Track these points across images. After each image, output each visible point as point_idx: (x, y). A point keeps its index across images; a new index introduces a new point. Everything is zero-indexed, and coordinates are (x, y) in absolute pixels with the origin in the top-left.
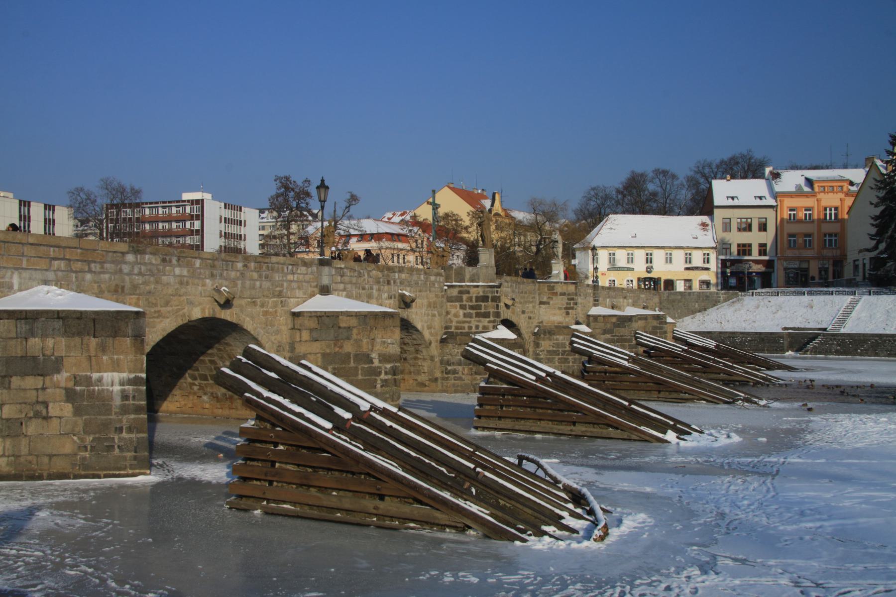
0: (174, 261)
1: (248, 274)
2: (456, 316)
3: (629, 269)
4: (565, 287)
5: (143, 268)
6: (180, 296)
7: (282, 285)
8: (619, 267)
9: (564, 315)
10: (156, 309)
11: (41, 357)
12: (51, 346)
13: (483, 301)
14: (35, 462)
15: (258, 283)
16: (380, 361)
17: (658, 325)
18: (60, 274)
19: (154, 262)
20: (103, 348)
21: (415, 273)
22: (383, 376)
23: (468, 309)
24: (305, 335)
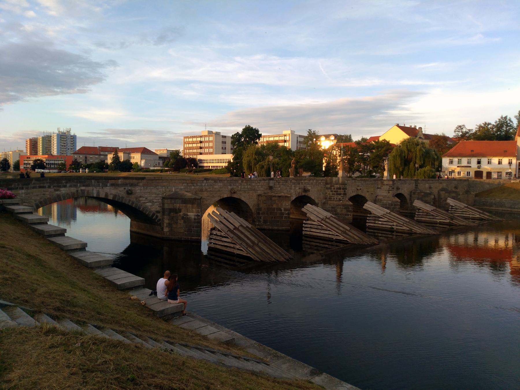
2: (329, 194)
7: (255, 187)
9: (388, 193)
15: (246, 187)
22: (285, 215)
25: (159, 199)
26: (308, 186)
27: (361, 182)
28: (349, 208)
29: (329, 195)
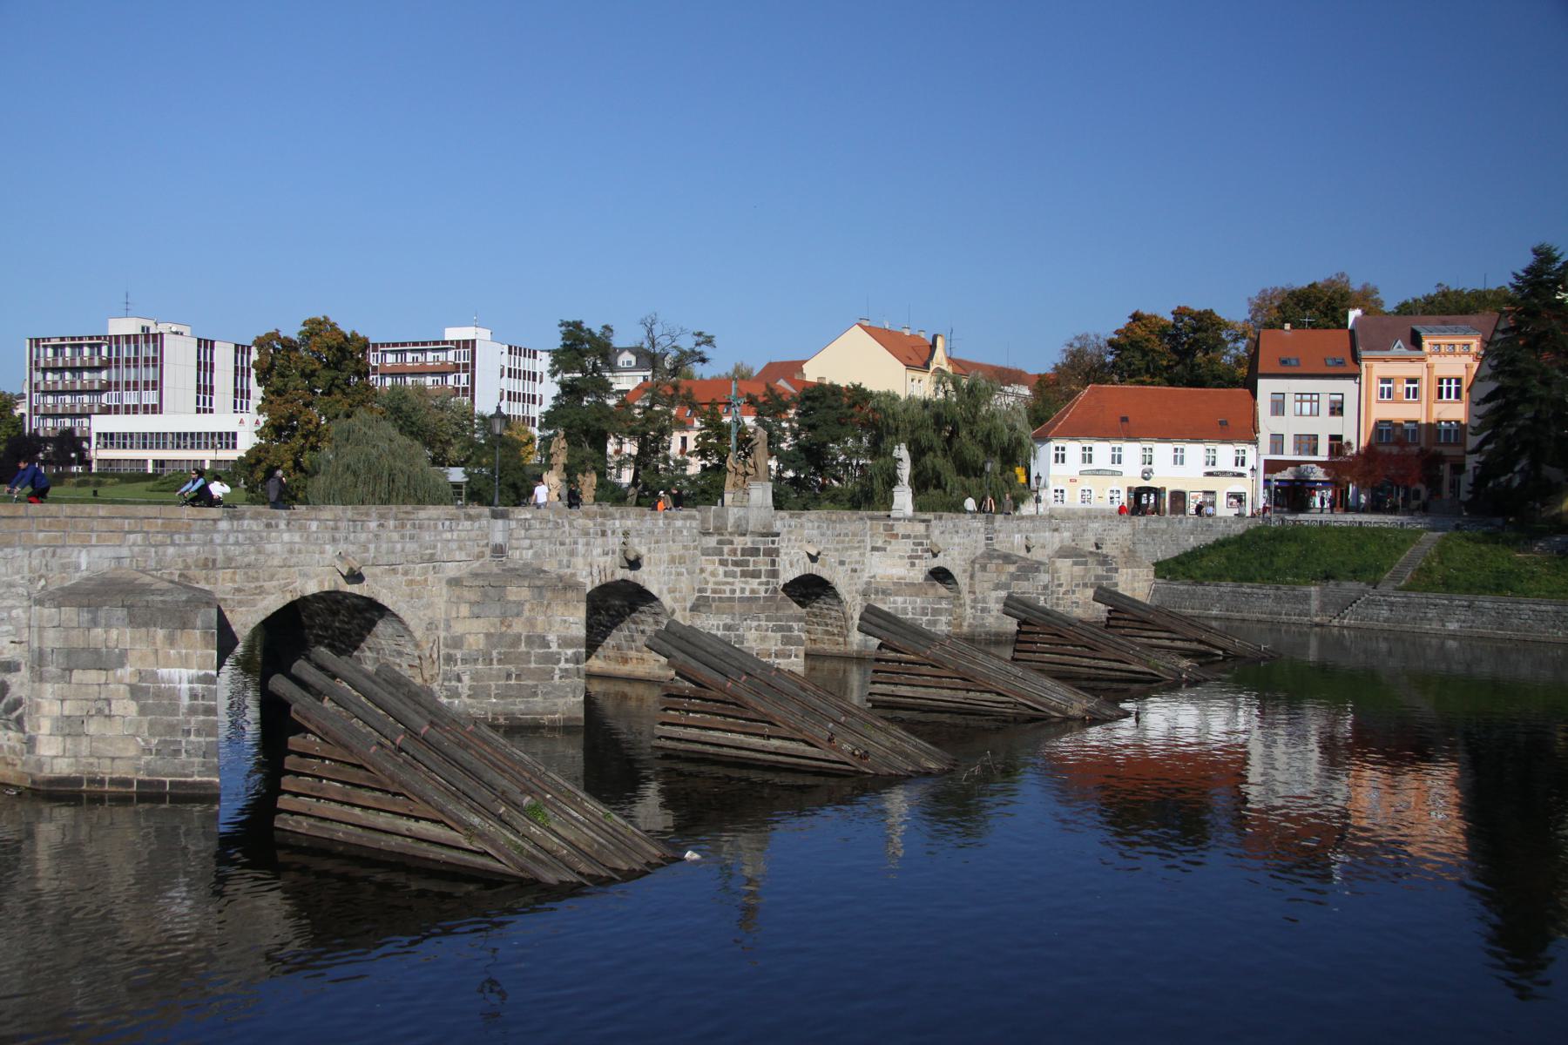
0: (282, 525)
1: (384, 535)
2: (713, 574)
3: (1114, 473)
5: (241, 536)
6: (289, 567)
7: (435, 547)
9: (908, 566)
10: (257, 584)
11: (104, 650)
12: (115, 637)
13: (752, 555)
14: (96, 764)
15: (399, 547)
16: (559, 646)
17: (1105, 573)
18: (136, 549)
19: (255, 528)
20: (171, 641)
22: (563, 665)
24: (465, 610)
25: (13, 607)
28: (790, 629)
29: (712, 580)
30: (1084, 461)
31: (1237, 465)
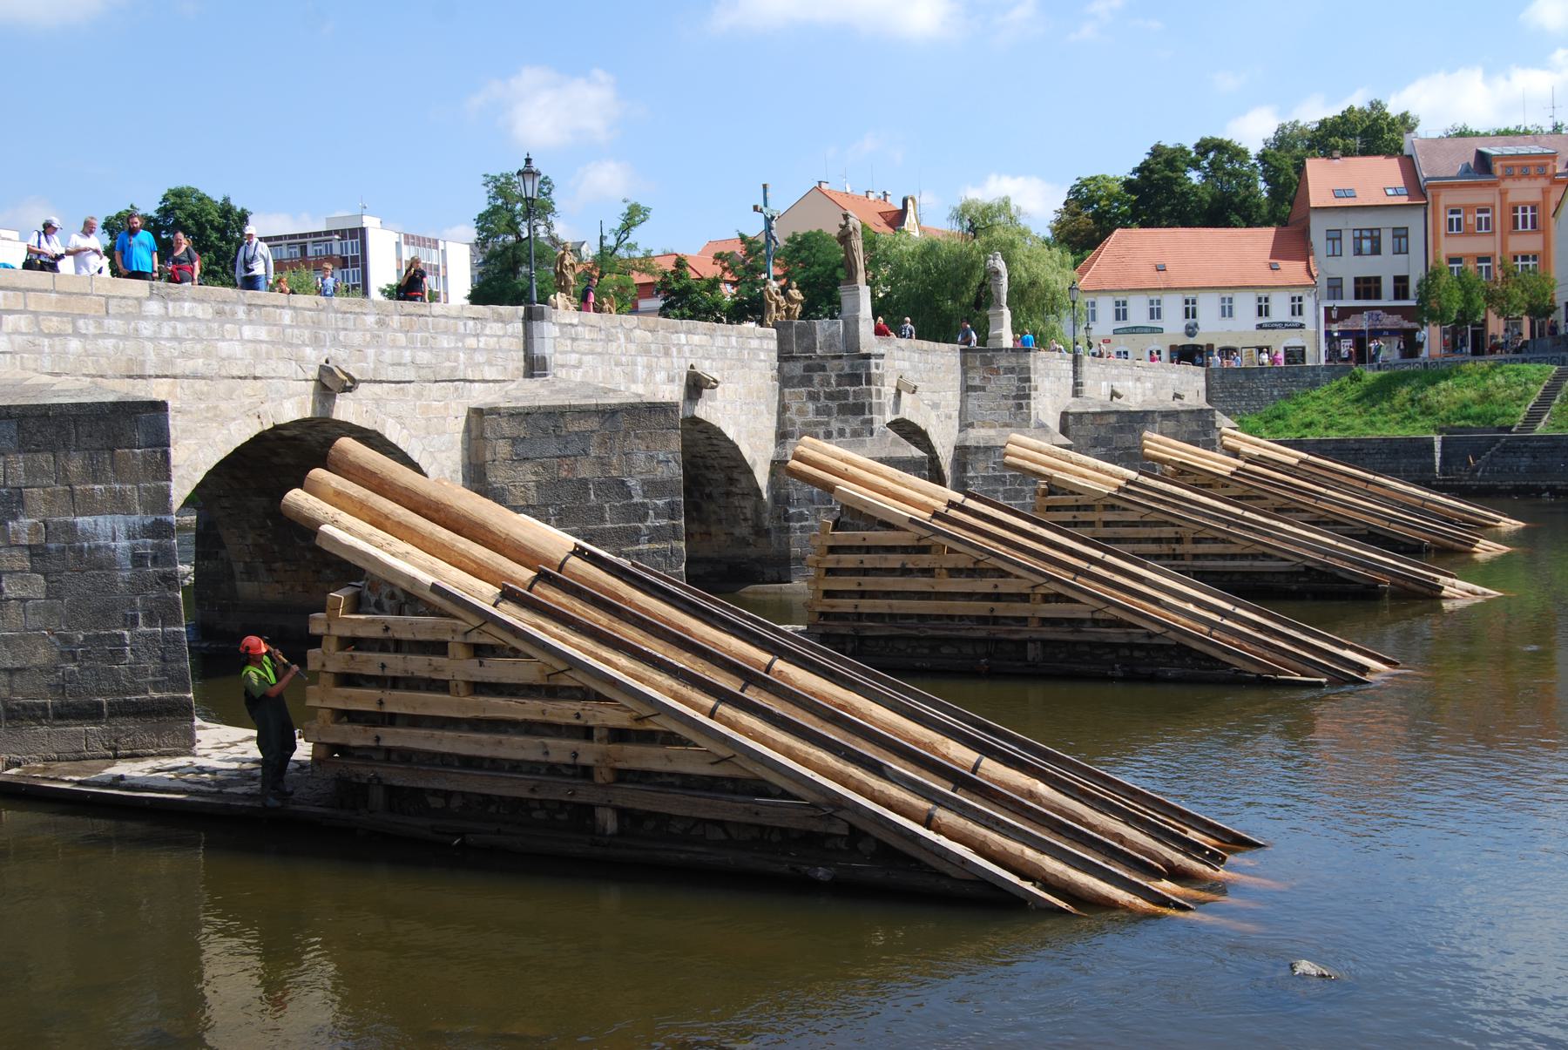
3: (1153, 330)
4: (1013, 360)
6: (255, 378)
8: (1135, 328)
13: (851, 385)
15: (407, 355)
18: (18, 339)
19: (200, 314)
21: (719, 333)
23: (822, 399)
24: (503, 448)
26: (707, 364)
27: (909, 359)
30: (1118, 318)
31: (1293, 314)
